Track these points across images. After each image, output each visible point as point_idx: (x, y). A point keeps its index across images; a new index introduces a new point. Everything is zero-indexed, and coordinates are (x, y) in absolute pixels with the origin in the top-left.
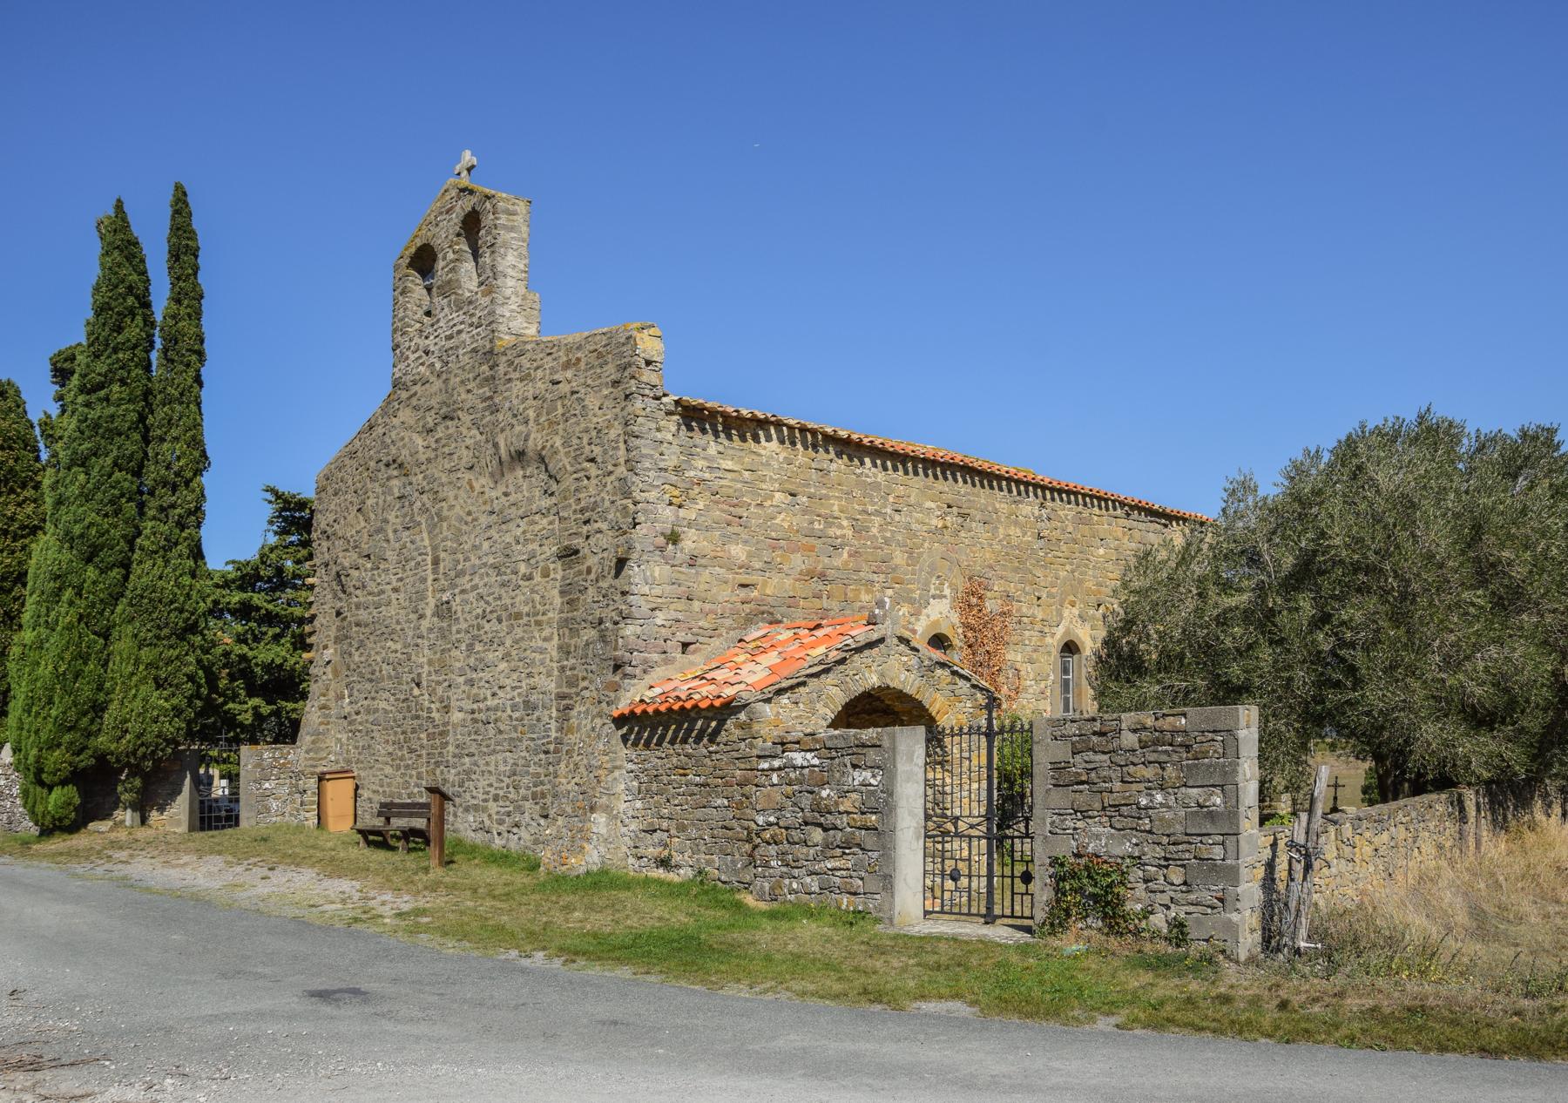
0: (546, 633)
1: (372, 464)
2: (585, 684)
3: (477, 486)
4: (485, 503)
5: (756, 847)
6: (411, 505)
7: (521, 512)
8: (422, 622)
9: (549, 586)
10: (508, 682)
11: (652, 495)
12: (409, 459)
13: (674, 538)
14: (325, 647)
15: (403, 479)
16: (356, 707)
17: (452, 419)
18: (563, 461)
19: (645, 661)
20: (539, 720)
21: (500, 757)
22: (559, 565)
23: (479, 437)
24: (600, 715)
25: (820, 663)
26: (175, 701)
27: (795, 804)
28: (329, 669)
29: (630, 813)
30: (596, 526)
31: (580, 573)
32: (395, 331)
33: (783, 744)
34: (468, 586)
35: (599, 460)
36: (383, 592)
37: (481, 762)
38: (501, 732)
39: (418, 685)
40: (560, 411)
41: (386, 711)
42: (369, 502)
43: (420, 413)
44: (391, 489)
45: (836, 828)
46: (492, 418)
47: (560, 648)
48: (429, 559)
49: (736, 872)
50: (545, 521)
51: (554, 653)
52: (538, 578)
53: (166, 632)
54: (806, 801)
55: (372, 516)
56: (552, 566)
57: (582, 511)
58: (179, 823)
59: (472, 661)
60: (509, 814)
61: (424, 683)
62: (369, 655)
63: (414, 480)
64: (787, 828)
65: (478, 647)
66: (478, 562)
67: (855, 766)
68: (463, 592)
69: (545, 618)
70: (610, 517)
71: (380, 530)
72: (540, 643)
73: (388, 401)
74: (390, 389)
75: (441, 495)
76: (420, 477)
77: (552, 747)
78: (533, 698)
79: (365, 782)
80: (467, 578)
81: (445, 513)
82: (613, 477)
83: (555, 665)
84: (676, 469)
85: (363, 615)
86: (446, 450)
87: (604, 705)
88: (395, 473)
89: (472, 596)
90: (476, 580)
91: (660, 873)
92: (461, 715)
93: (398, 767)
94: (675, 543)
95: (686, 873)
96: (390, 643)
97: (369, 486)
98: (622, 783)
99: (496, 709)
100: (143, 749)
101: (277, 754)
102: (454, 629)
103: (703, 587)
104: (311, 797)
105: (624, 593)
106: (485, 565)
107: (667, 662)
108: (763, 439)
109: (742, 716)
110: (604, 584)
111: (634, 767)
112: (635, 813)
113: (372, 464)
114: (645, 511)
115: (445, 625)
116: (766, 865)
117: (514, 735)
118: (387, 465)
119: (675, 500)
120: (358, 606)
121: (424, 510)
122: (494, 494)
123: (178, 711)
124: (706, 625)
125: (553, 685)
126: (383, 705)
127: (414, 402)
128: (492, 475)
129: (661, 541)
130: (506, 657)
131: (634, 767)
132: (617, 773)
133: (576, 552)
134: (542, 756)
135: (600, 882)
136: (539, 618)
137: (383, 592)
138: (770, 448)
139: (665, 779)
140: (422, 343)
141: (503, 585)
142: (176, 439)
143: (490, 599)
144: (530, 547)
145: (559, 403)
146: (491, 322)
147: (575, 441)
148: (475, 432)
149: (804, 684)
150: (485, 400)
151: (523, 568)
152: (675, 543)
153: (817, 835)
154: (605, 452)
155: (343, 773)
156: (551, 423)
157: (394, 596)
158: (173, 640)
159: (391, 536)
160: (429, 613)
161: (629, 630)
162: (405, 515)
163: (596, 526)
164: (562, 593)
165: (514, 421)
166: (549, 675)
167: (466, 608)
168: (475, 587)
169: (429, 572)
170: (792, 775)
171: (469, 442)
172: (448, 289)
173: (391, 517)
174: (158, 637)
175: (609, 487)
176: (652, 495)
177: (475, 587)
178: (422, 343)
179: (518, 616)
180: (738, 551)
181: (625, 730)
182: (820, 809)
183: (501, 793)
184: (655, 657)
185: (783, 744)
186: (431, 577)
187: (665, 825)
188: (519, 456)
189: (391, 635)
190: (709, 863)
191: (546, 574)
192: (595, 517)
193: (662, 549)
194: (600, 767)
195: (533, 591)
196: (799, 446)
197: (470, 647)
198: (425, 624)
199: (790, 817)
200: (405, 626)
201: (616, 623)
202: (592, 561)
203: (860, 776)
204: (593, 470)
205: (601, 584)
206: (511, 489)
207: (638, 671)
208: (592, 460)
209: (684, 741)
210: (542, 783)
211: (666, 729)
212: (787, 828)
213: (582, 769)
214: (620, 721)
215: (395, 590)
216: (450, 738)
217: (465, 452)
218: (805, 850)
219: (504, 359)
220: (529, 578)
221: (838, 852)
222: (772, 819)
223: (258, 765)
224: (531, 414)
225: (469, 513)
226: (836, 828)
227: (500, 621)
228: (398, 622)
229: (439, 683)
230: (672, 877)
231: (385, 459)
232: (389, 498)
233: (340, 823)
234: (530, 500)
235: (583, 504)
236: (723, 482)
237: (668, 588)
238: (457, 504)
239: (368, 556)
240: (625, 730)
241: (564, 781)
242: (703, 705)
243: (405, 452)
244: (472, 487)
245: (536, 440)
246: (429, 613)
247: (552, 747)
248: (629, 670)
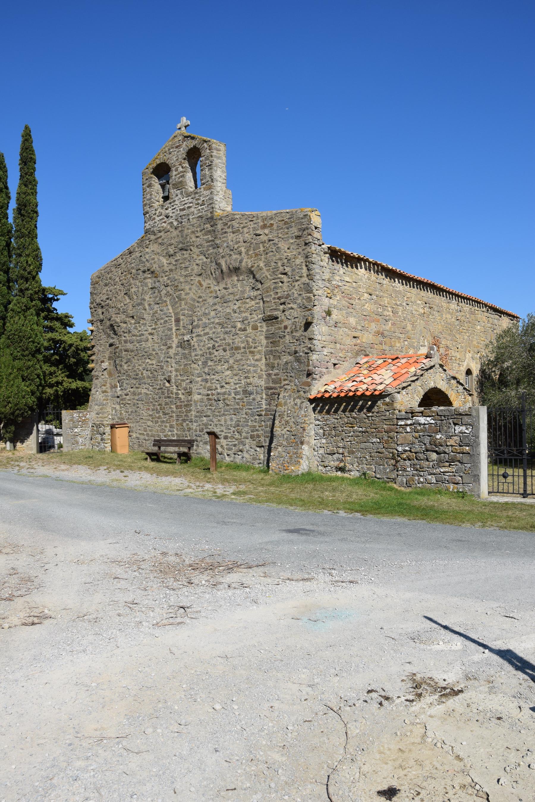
0: (258, 357)
1: (134, 271)
2: (286, 382)
3: (205, 284)
4: (211, 292)
5: (397, 462)
6: (159, 292)
7: (237, 297)
8: (170, 350)
9: (258, 334)
10: (231, 380)
11: (320, 292)
12: (158, 269)
13: (329, 313)
14: (103, 362)
15: (154, 279)
16: (125, 392)
17: (186, 250)
18: (266, 273)
19: (321, 372)
20: (254, 399)
21: (228, 417)
22: (264, 324)
23: (205, 260)
24: (299, 397)
25: (415, 375)
26: (32, 387)
27: (420, 441)
28: (105, 373)
29: (319, 445)
30: (289, 306)
31: (280, 328)
32: (145, 205)
33: (412, 413)
34: (202, 333)
35: (289, 274)
36: (143, 335)
37: (214, 420)
38: (228, 405)
39: (169, 382)
40: (262, 249)
41: (147, 394)
42: (133, 290)
43: (164, 247)
44: (146, 285)
45: (445, 453)
46: (215, 250)
47: (267, 365)
48: (173, 319)
49: (386, 473)
50: (253, 303)
51: (263, 367)
52: (249, 330)
53: (27, 352)
54: (427, 440)
55: (135, 297)
56: (259, 325)
57: (279, 298)
58: (31, 449)
59: (206, 370)
60: (235, 445)
61: (173, 381)
62: (134, 366)
63: (161, 280)
64: (416, 453)
65: (210, 363)
66: (207, 321)
67: (455, 424)
68: (198, 336)
69: (255, 350)
70: (299, 301)
71: (139, 304)
72: (253, 362)
73: (142, 240)
74: (143, 234)
75: (180, 288)
76: (166, 278)
77: (263, 413)
78: (250, 389)
79: (134, 429)
80: (201, 329)
81: (183, 296)
82: (299, 283)
83: (264, 373)
84: (329, 281)
85: (129, 346)
86: (183, 265)
87: (302, 393)
88: (149, 276)
89: (204, 338)
90: (207, 330)
91: (339, 474)
92: (200, 397)
93: (157, 422)
94: (329, 316)
95: (355, 474)
96: (148, 360)
97: (132, 281)
98: (312, 430)
99: (224, 393)
100: (18, 412)
101: (81, 415)
102: (193, 354)
103: (340, 337)
104: (107, 437)
105: (310, 339)
106: (213, 323)
107: (329, 372)
108: (359, 268)
109: (387, 400)
110: (297, 334)
111: (320, 423)
112: (322, 445)
113: (134, 271)
114: (318, 300)
115: (186, 352)
116: (405, 470)
117: (238, 407)
118: (144, 272)
119: (328, 295)
120: (126, 342)
121: (168, 294)
122: (217, 288)
123: (33, 393)
124: (342, 356)
125: (263, 383)
126: (144, 391)
127: (160, 241)
128: (216, 279)
129: (324, 314)
130: (231, 368)
131: (320, 423)
132: (311, 426)
133: (277, 318)
134: (257, 417)
135: (309, 477)
136: (252, 349)
137: (143, 335)
138: (362, 271)
139: (340, 429)
140: (164, 212)
141: (226, 333)
142: (28, 255)
143: (218, 340)
144: (244, 315)
145: (261, 245)
146: (211, 203)
147: (273, 264)
148: (202, 257)
149: (410, 385)
150: (209, 242)
151: (239, 325)
152: (329, 316)
153: (434, 456)
154: (293, 270)
155: (123, 425)
156: (256, 255)
157: (150, 337)
158: (30, 357)
159: (147, 307)
160: (174, 346)
161: (314, 357)
162: (156, 297)
163: (289, 306)
164: (267, 338)
165: (232, 253)
166: (260, 377)
167: (200, 345)
168: (206, 334)
169: (173, 325)
170: (419, 428)
171: (198, 262)
172: (180, 185)
173: (147, 298)
174: (23, 356)
175: (296, 287)
176: (320, 292)
177: (207, 334)
178: (164, 212)
179: (238, 348)
180: (352, 321)
181: (314, 405)
182: (434, 443)
183: (229, 435)
184: (324, 370)
185: (412, 413)
186: (174, 328)
187: (341, 451)
188: (236, 270)
189: (149, 357)
190: (368, 469)
191: (255, 328)
192: (288, 301)
193: (324, 318)
194: (304, 423)
195: (246, 336)
196: (372, 271)
197: (205, 363)
198: (172, 352)
199: (417, 447)
200: (159, 352)
201: (307, 353)
202: (287, 323)
203: (458, 429)
204: (285, 278)
205: (294, 334)
206: (229, 286)
207: (317, 377)
208: (285, 274)
209: (352, 411)
210: (257, 430)
211: (340, 405)
212: (416, 453)
213: (291, 424)
214: (311, 401)
215: (151, 334)
216: (193, 408)
217: (196, 267)
218: (427, 463)
219: (221, 222)
220: (245, 330)
221: (447, 464)
222: (407, 448)
223: (72, 420)
224: (243, 250)
225: (200, 297)
226: (445, 453)
227: (225, 350)
228: (154, 350)
229: (183, 381)
230: (346, 475)
231: (142, 269)
232: (145, 288)
233: (123, 449)
234: (243, 292)
235: (279, 295)
236: (346, 287)
237: (328, 337)
238: (191, 292)
239: (133, 317)
240: (314, 405)
241: (278, 429)
242: (368, 393)
243: (154, 266)
244: (201, 285)
245: (247, 262)
246: (174, 346)
247: (263, 413)
248: (314, 376)
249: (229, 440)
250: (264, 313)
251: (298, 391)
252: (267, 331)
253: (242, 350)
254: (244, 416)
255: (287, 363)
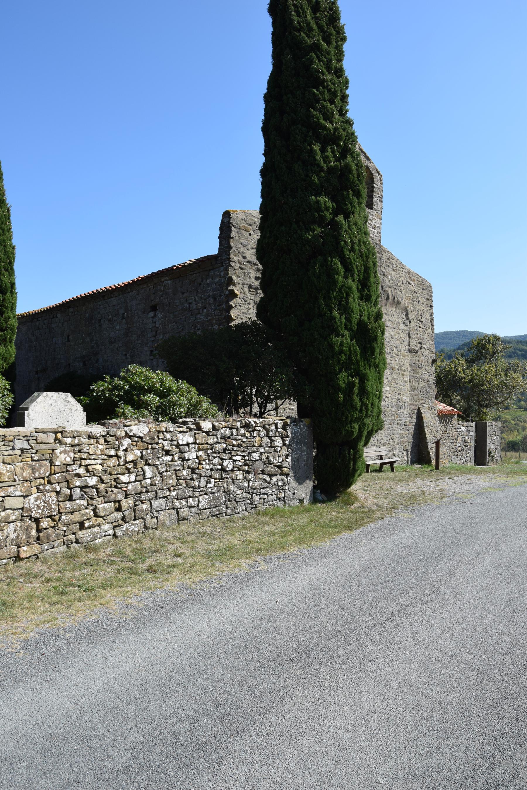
2: (423, 401)
22: (409, 354)
35: (424, 322)
47: (411, 386)
151: (395, 350)
164: (411, 366)
208: (421, 322)
247: (408, 423)
249: (387, 447)
250: (409, 345)
251: (432, 409)
252: (411, 360)
253: (397, 371)
254: (396, 426)
255: (422, 387)
